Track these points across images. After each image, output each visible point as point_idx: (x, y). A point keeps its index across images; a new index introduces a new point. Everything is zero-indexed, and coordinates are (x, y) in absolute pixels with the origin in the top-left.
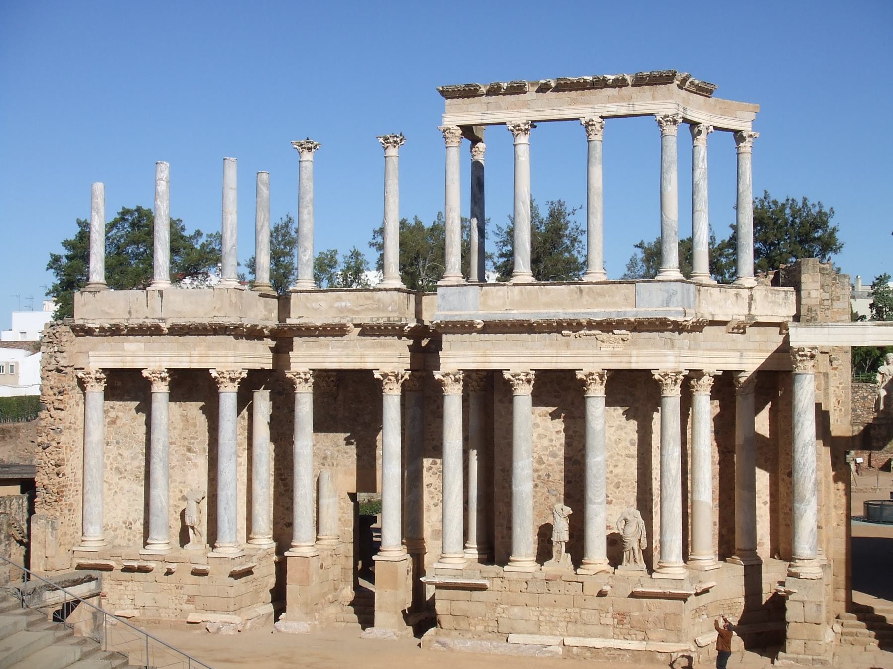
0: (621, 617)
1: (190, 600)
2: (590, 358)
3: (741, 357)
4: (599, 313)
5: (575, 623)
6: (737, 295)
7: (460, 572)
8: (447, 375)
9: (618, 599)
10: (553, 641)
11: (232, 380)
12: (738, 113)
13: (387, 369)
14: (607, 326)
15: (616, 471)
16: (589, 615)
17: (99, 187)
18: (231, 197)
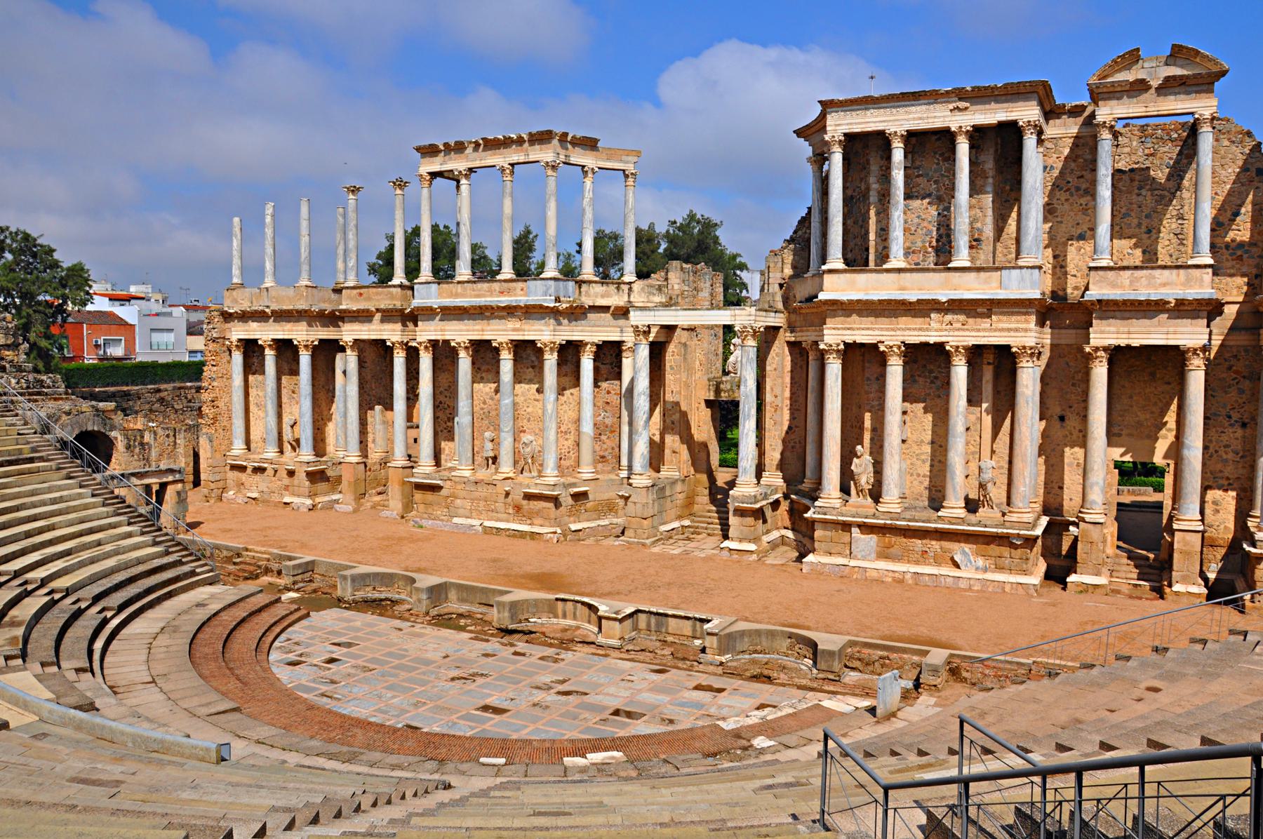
0: (518, 508)
1: (287, 488)
2: (501, 332)
3: (622, 331)
4: (504, 300)
5: (492, 512)
6: (618, 289)
7: (428, 476)
8: (420, 343)
9: (517, 496)
10: (476, 522)
11: (306, 346)
12: (624, 158)
13: (394, 339)
14: (510, 311)
15: (529, 410)
16: (500, 506)
17: (236, 220)
18: (304, 224)
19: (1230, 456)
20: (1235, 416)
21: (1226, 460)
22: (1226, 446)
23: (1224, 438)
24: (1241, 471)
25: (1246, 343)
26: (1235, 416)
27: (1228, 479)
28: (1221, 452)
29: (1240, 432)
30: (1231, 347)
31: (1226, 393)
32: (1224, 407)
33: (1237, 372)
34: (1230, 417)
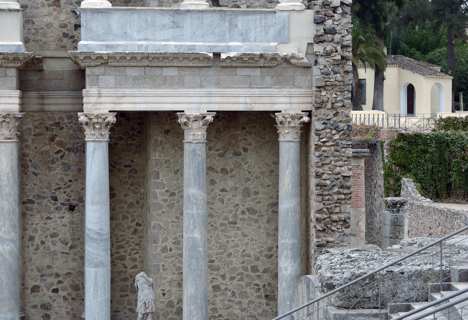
19: (59, 247)
20: (62, 197)
21: (54, 253)
22: (54, 235)
23: (51, 224)
24: (72, 265)
25: (70, 108)
26: (62, 197)
27: (57, 275)
28: (49, 243)
29: (68, 216)
30: (52, 112)
31: (50, 169)
32: (49, 187)
33: (60, 144)
34: (55, 199)
